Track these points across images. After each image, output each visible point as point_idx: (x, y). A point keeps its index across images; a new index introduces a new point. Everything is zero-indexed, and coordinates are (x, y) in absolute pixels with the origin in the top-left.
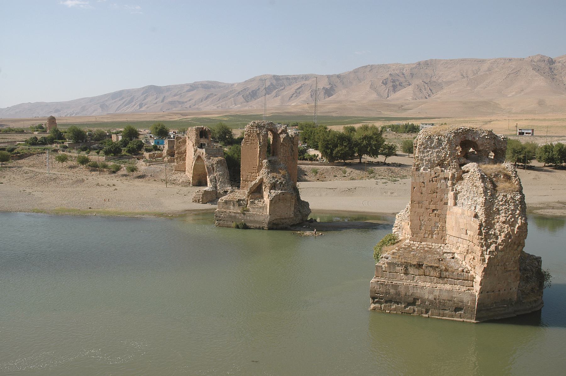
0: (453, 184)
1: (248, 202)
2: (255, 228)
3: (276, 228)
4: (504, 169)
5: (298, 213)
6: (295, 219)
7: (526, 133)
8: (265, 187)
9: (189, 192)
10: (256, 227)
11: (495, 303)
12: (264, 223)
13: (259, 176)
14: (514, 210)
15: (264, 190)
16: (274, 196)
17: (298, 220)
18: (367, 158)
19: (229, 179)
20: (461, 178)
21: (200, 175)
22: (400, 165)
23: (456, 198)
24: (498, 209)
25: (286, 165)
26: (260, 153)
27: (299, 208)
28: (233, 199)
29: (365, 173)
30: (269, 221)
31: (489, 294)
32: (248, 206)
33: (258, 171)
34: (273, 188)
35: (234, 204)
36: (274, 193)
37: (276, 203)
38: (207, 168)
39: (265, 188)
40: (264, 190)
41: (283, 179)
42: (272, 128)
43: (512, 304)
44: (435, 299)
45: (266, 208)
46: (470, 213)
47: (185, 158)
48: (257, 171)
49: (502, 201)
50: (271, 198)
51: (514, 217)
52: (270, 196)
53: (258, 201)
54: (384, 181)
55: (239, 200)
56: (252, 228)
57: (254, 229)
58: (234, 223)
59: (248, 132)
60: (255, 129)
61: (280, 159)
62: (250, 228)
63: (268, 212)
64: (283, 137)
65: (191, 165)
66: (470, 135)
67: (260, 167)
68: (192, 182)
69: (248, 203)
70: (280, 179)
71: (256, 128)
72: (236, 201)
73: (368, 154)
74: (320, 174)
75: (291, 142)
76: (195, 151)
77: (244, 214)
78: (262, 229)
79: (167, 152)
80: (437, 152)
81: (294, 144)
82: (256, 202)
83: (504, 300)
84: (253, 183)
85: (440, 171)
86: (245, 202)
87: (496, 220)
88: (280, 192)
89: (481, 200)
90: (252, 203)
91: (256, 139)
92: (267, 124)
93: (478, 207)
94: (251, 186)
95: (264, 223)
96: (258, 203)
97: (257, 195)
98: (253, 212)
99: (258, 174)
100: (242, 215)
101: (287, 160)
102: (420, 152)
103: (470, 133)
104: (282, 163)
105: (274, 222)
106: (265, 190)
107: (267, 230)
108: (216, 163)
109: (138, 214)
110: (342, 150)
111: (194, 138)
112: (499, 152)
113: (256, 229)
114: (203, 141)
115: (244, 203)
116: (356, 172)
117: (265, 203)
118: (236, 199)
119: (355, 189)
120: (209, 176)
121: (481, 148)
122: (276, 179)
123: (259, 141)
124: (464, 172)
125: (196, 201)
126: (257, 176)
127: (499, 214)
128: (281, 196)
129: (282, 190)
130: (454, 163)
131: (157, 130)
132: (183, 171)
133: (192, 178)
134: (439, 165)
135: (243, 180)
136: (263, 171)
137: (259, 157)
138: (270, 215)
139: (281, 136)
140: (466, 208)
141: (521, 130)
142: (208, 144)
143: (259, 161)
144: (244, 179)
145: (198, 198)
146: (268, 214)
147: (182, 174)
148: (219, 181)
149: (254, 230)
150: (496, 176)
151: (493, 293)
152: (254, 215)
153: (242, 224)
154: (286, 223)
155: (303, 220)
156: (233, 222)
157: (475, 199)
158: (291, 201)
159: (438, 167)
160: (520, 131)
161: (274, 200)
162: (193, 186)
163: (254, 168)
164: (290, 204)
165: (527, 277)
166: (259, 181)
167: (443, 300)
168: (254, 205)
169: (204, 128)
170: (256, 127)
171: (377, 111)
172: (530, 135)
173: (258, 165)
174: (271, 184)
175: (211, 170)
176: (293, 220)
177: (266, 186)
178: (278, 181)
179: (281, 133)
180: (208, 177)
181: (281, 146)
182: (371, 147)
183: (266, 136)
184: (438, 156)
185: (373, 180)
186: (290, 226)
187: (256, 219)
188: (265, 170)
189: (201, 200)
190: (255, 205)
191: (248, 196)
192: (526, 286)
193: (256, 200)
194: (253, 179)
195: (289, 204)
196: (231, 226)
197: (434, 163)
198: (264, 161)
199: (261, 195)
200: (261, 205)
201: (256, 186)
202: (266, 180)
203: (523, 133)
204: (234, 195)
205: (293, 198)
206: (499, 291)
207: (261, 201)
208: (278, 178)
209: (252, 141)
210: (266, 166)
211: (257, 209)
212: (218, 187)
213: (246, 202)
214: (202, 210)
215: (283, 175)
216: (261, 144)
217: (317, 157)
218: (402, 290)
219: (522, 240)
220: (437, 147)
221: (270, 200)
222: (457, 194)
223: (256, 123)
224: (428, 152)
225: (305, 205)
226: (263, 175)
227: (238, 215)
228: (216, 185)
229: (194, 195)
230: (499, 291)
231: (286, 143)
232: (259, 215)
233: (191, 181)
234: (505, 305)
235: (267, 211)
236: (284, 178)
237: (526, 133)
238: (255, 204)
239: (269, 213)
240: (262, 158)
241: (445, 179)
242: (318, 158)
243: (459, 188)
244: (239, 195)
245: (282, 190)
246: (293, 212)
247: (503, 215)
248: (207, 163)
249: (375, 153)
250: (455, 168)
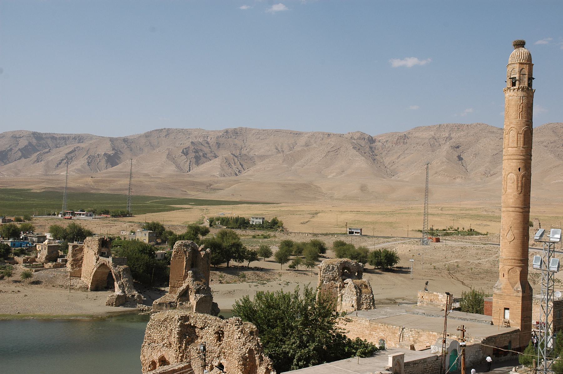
0: (340, 290)
4: (364, 282)
7: (356, 233)
9: (97, 297)
14: (370, 303)
18: (233, 263)
20: (344, 287)
21: (97, 281)
22: (262, 270)
23: (342, 297)
24: (362, 302)
29: (236, 278)
32: (177, 306)
35: (166, 305)
36: (199, 296)
38: (115, 275)
39: (191, 293)
41: (204, 286)
45: (193, 308)
46: (350, 305)
47: (81, 265)
48: (182, 279)
49: (364, 298)
51: (370, 306)
54: (255, 284)
55: (170, 303)
65: (90, 271)
67: (186, 276)
68: (91, 287)
70: (203, 286)
71: (184, 247)
73: (235, 259)
76: (98, 259)
79: (46, 257)
80: (332, 273)
82: (184, 303)
84: (181, 289)
85: (333, 283)
87: (362, 308)
89: (355, 298)
90: (181, 304)
93: (354, 302)
97: (184, 298)
102: (323, 273)
106: (191, 295)
108: (122, 271)
109: (71, 316)
110: (216, 256)
111: (96, 248)
114: (104, 250)
116: (228, 277)
119: (234, 291)
120: (117, 282)
121: (352, 271)
122: (200, 286)
124: (345, 284)
125: (109, 304)
127: (363, 305)
128: (204, 299)
130: (340, 279)
131: (11, 231)
132: (78, 277)
133: (90, 284)
134: (333, 280)
136: (189, 280)
139: (201, 252)
140: (347, 302)
141: (351, 229)
142: (107, 253)
144: (172, 285)
145: (112, 302)
147: (78, 280)
148: (126, 286)
150: (361, 285)
157: (352, 297)
159: (333, 281)
160: (350, 230)
162: (91, 291)
169: (105, 239)
171: (182, 191)
172: (359, 234)
174: (197, 290)
175: (119, 278)
179: (201, 250)
180: (115, 283)
182: (239, 254)
184: (332, 275)
185: (245, 283)
188: (190, 278)
189: (114, 304)
191: (178, 299)
197: (330, 279)
203: (353, 233)
207: (188, 303)
212: (126, 292)
214: (120, 312)
220: (332, 271)
222: (342, 295)
224: (327, 273)
226: (189, 282)
228: (124, 290)
229: (108, 299)
231: (205, 258)
233: (89, 286)
236: (204, 284)
237: (356, 233)
241: (337, 287)
243: (343, 292)
247: (365, 305)
248: (114, 271)
249: (241, 258)
250: (340, 281)
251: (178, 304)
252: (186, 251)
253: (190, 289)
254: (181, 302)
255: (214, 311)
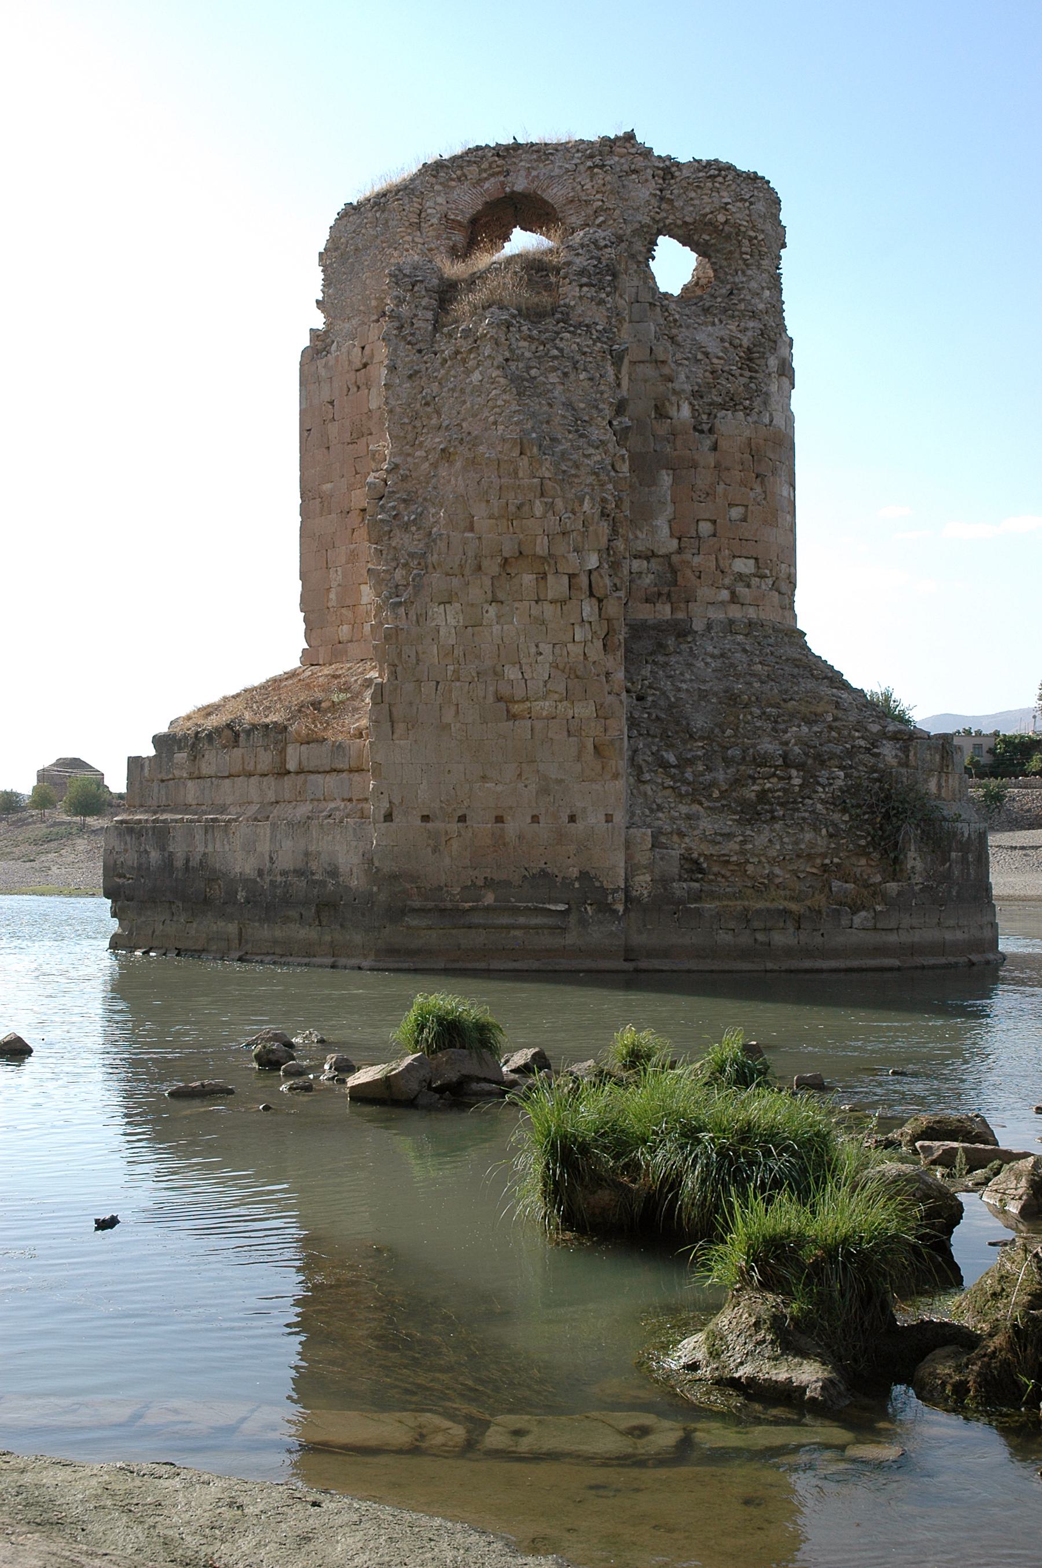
11: (490, 883)
31: (429, 825)
43: (604, 908)
44: (260, 873)
66: (523, 173)
83: (544, 874)
103: (523, 164)
112: (707, 241)
151: (454, 827)
165: (762, 795)
167: (281, 875)
192: (743, 842)
206: (499, 819)
218: (178, 848)
219: (539, 541)
230: (499, 819)
234: (556, 901)
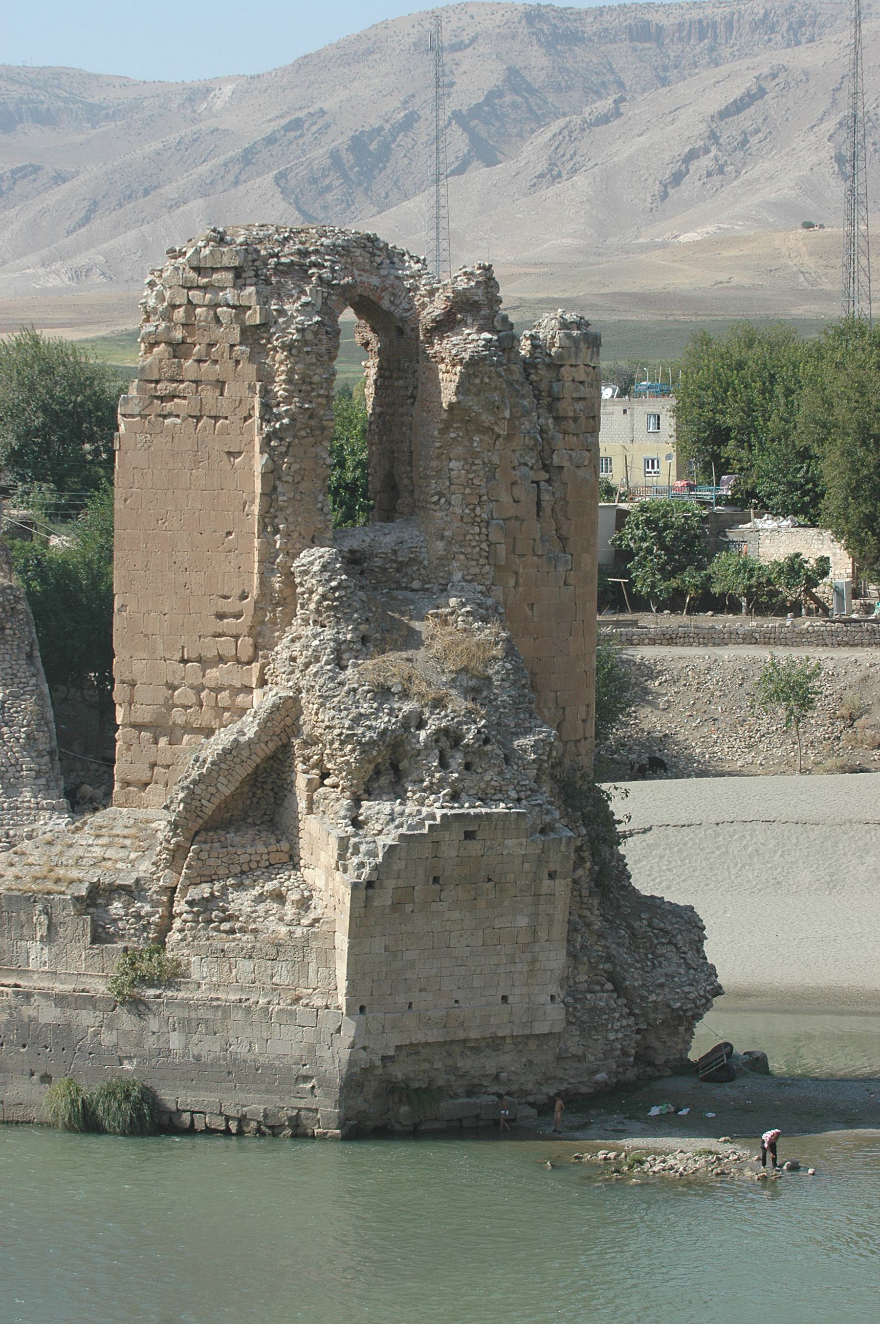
1: (177, 909)
2: (233, 1126)
3: (416, 1126)
5: (603, 999)
6: (573, 1045)
8: (315, 774)
10: (242, 1120)
12: (306, 1078)
13: (263, 682)
15: (302, 805)
16: (391, 850)
17: (606, 1054)
19: (51, 753)
25: (498, 591)
26: (270, 494)
27: (609, 958)
28: (50, 885)
30: (351, 1063)
32: (174, 936)
33: (256, 647)
34: (384, 780)
37: (409, 908)
39: (312, 787)
40: (302, 805)
41: (458, 704)
42: (375, 281)
45: (327, 956)
48: (245, 643)
50: (361, 865)
52: (356, 852)
53: (260, 899)
56: (209, 1131)
57: (227, 1132)
58: (59, 1086)
59: (167, 316)
60: (229, 295)
61: (440, 545)
62: (190, 1131)
63: (342, 984)
64: (466, 356)
69: (171, 917)
70: (438, 703)
72: (77, 899)
74: (833, 717)
75: (538, 397)
77: (137, 1006)
78: (294, 1136)
81: (557, 419)
84: (223, 739)
86: (148, 908)
88: (439, 813)
91: (237, 377)
92: (333, 249)
94: (195, 774)
95: (306, 1078)
96: (261, 908)
98: (216, 987)
99: (256, 666)
100: (126, 1020)
101: (502, 550)
104: (458, 576)
105: (398, 1072)
106: (310, 810)
107: (334, 1138)
113: (240, 1133)
115: (138, 917)
117: (312, 915)
118: (72, 882)
122: (407, 707)
123: (266, 392)
126: (248, 690)
129: (455, 797)
135: (134, 726)
136: (298, 645)
137: (263, 526)
138: (362, 1009)
143: (267, 559)
144: (144, 713)
146: (342, 1000)
149: (221, 1142)
152: (226, 1011)
153: (127, 1096)
154: (497, 1078)
155: (651, 1064)
156: (46, 1078)
158: (537, 895)
161: (390, 884)
163: (221, 616)
164: (535, 916)
166: (264, 726)
168: (226, 926)
170: (238, 272)
173: (255, 592)
174: (365, 748)
176: (559, 1058)
177: (319, 764)
178: (421, 725)
181: (444, 431)
183: (323, 349)
186: (532, 1105)
187: (240, 1050)
188: (309, 631)
190: (232, 931)
191: (176, 856)
193: (240, 886)
194: (219, 710)
195: (523, 921)
196: (34, 1114)
198: (305, 557)
199: (285, 846)
200: (283, 930)
201: (243, 772)
202: (325, 716)
204: (57, 849)
205: (552, 867)
207: (279, 897)
208: (421, 695)
209: (208, 394)
210: (324, 597)
211: (246, 965)
213: (155, 904)
215: (464, 670)
216: (278, 417)
217: (812, 582)
221: (355, 886)
223: (232, 242)
225: (666, 932)
227: (87, 1018)
231: (495, 408)
232: (265, 1010)
235: (332, 976)
236: (473, 693)
238: (230, 918)
239: (351, 992)
240: (288, 535)
242: (822, 590)
244: (98, 852)
245: (455, 797)
246: (554, 989)
251: (180, 906)
252: (265, 325)
253: (306, 744)
254: (205, 890)
255: (619, 989)
